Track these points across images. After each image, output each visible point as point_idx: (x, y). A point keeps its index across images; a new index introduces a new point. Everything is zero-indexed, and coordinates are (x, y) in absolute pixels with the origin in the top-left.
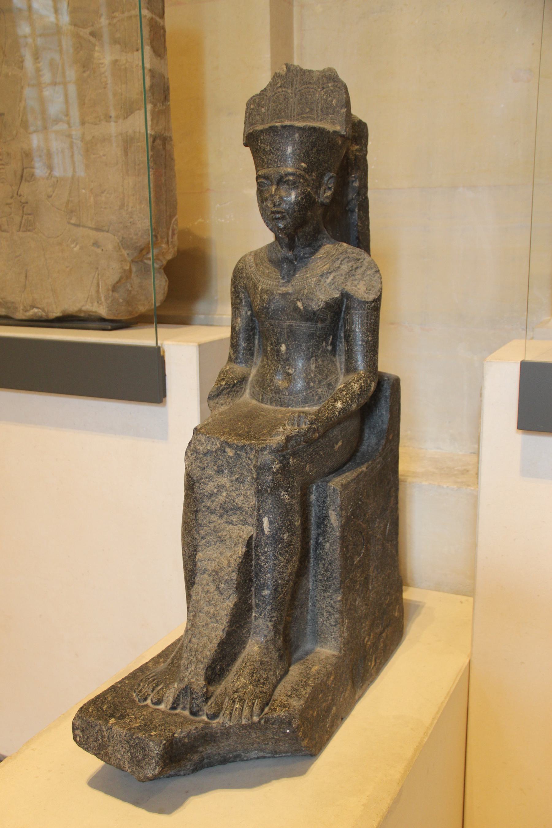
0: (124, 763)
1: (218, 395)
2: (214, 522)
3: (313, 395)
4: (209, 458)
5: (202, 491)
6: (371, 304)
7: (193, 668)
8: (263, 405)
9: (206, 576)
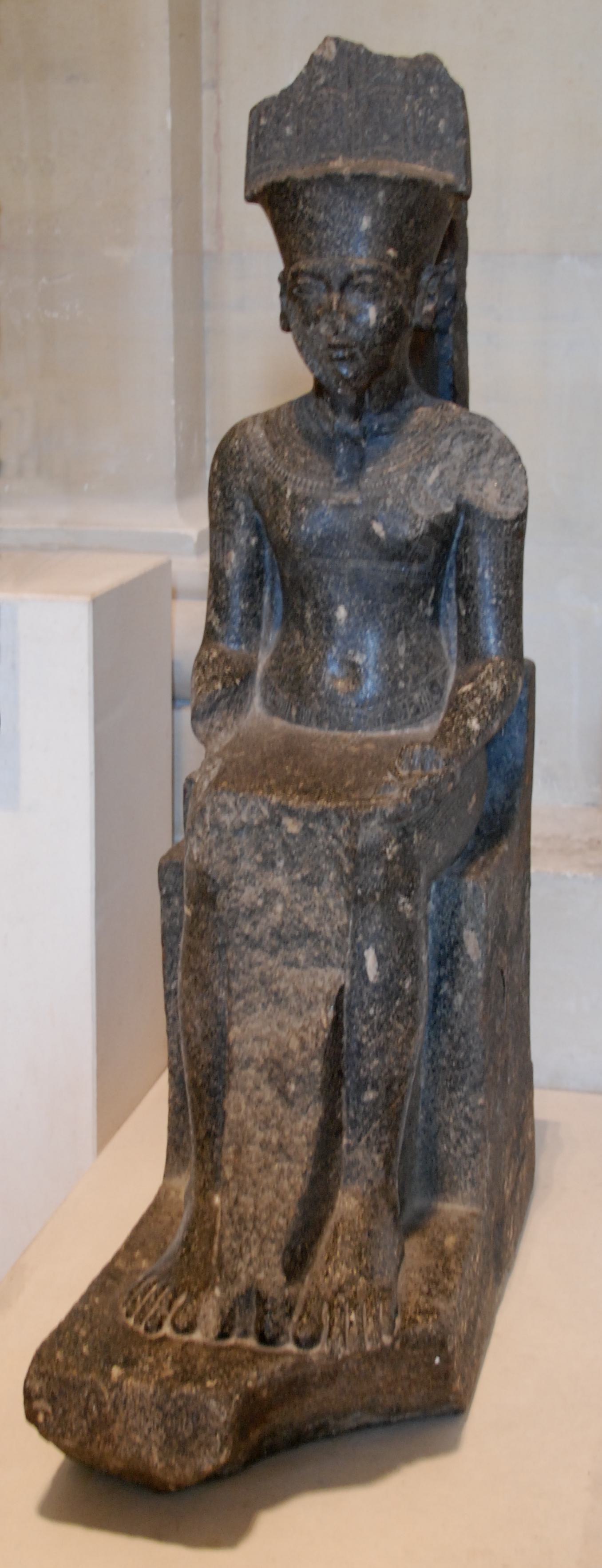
0: (150, 1452)
1: (211, 710)
2: (260, 964)
3: (404, 706)
4: (244, 838)
5: (233, 905)
6: (513, 525)
7: (254, 1252)
8: (301, 728)
9: (251, 1071)
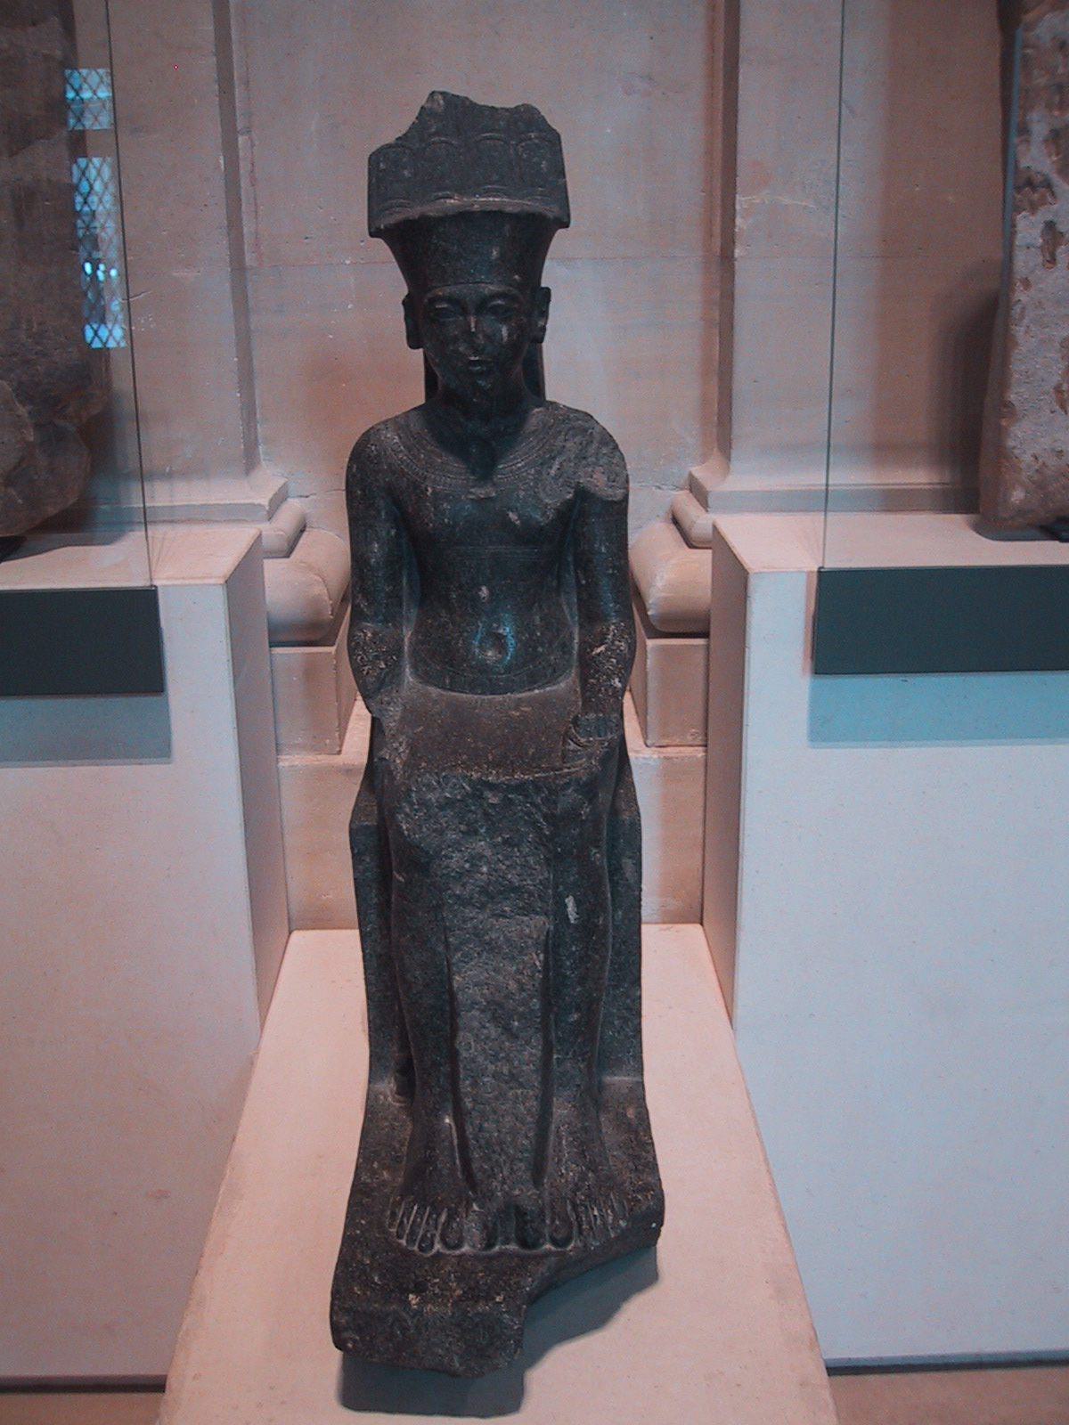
0: (452, 1360)
2: (472, 919)
7: (506, 1173)
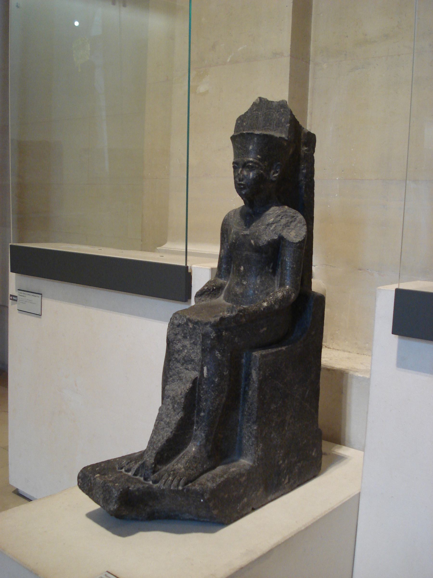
4: (180, 329)
9: (169, 400)
